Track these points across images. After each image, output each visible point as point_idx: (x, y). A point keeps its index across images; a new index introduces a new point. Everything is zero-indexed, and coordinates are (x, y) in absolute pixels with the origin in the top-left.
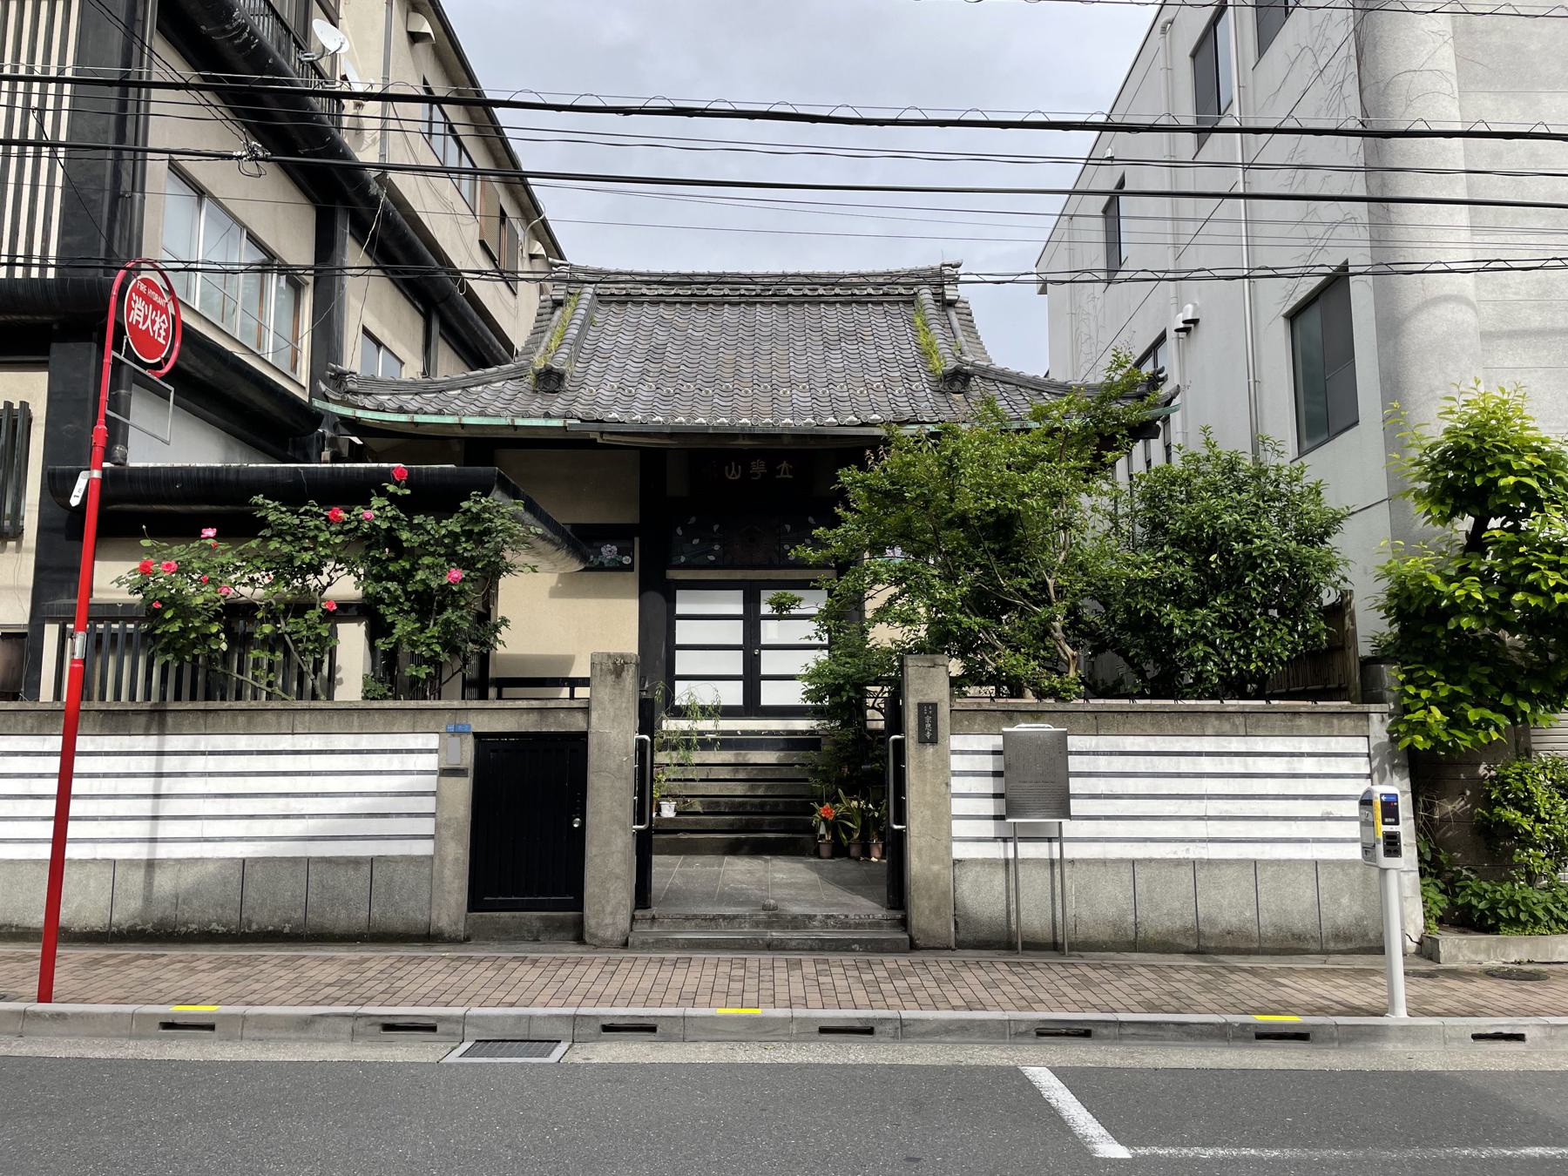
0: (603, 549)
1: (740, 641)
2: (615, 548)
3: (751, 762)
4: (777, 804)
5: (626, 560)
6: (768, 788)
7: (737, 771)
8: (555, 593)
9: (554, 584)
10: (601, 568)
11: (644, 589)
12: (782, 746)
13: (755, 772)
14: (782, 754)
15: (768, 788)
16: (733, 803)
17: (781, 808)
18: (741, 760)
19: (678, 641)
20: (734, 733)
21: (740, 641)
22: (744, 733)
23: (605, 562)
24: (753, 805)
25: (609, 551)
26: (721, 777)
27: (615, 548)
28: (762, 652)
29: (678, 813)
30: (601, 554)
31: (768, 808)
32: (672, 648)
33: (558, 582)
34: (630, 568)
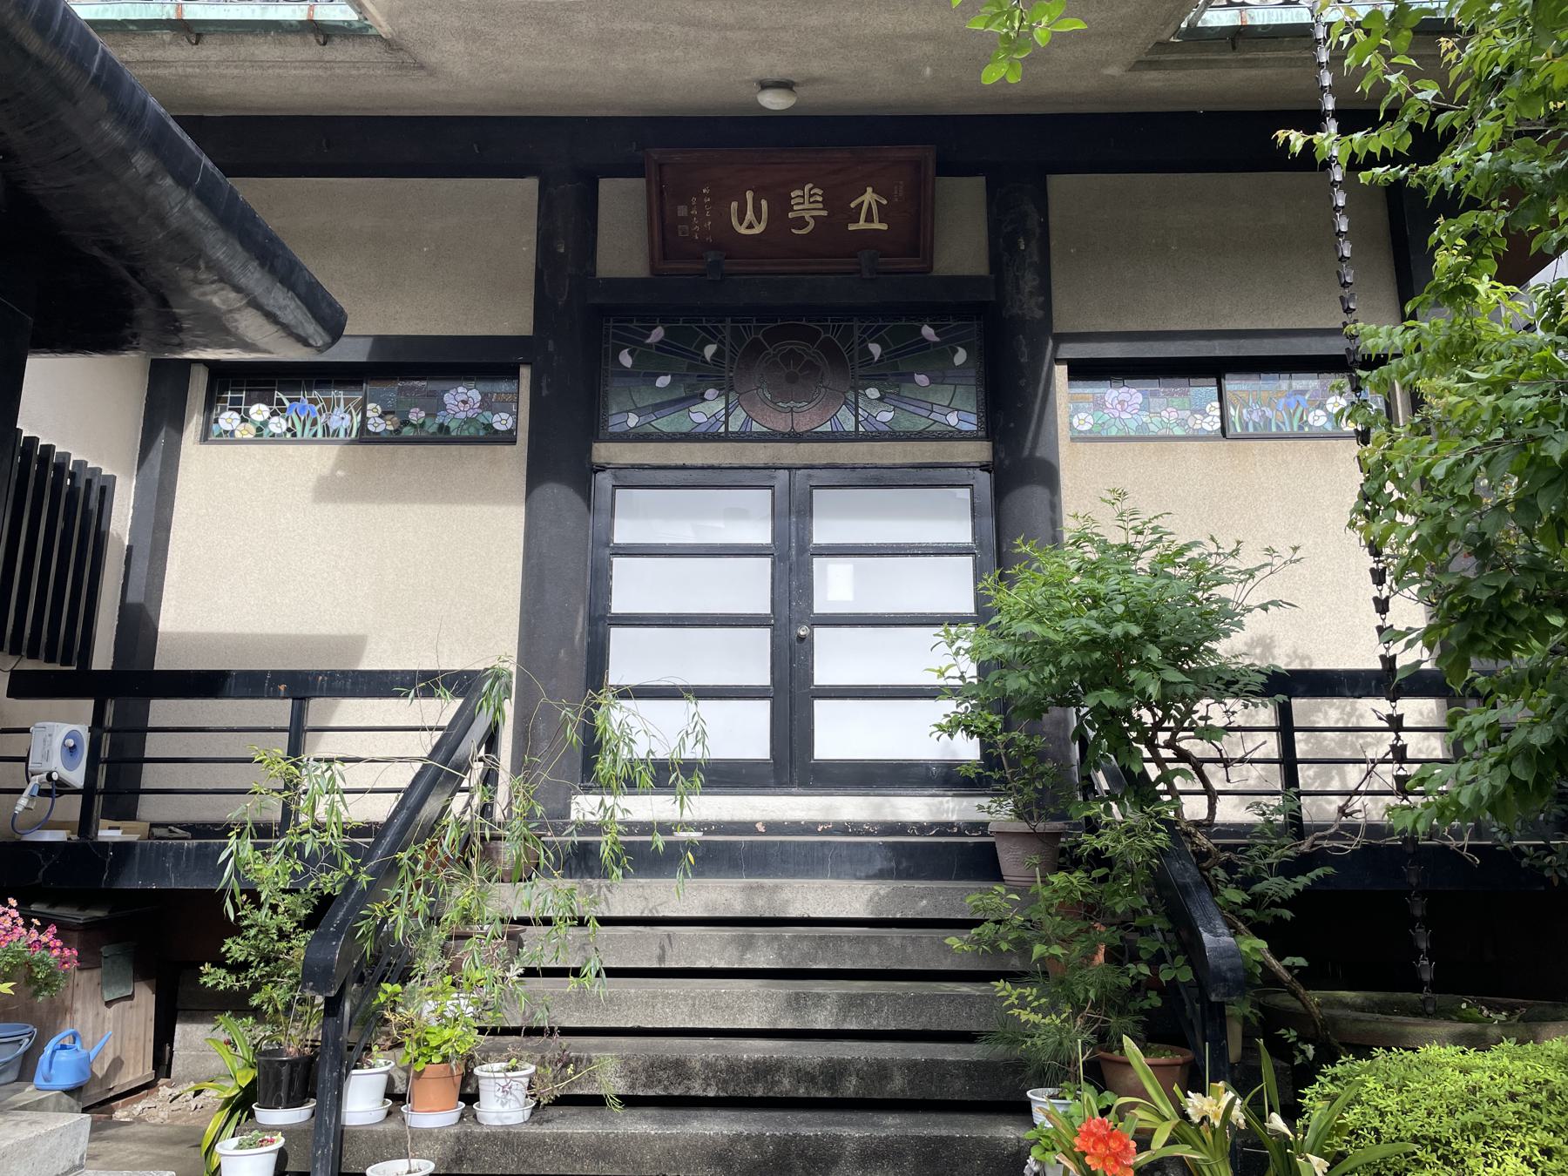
0: (447, 398)
1: (763, 606)
2: (475, 395)
3: (793, 913)
4: (881, 1070)
5: (502, 422)
6: (850, 1004)
7: (747, 945)
8: (328, 490)
9: (326, 471)
10: (443, 437)
11: (537, 474)
12: (879, 864)
13: (805, 946)
14: (884, 887)
15: (850, 1004)
16: (733, 1068)
17: (897, 1086)
18: (762, 908)
19: (618, 606)
20: (747, 827)
21: (763, 606)
22: (773, 827)
23: (453, 425)
24: (802, 1074)
25: (462, 400)
26: (702, 964)
27: (475, 395)
28: (817, 630)
29: (545, 1106)
30: (443, 407)
31: (850, 1087)
32: (601, 621)
33: (337, 466)
34: (509, 438)
